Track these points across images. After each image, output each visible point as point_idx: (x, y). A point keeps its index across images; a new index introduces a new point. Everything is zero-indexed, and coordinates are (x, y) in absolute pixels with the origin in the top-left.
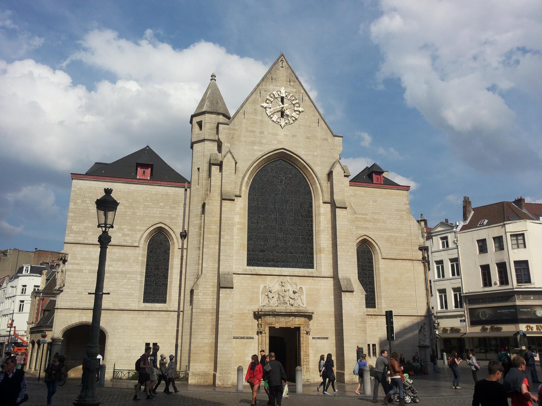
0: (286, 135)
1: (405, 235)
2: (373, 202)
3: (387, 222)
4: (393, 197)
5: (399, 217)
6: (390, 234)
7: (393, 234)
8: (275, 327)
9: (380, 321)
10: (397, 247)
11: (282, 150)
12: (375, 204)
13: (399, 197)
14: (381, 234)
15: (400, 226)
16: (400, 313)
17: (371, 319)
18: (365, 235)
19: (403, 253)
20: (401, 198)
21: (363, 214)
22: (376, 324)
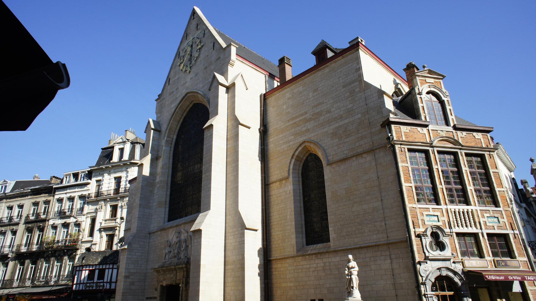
0: (191, 79)
1: (360, 116)
2: (313, 93)
3: (332, 110)
4: (338, 71)
5: (348, 94)
6: (337, 125)
7: (341, 123)
8: (163, 285)
9: (329, 262)
10: (347, 140)
11: (188, 95)
12: (315, 94)
13: (347, 66)
14: (325, 130)
15: (351, 106)
16: (358, 243)
17: (316, 260)
18: (304, 142)
19: (357, 144)
20: (351, 64)
21: (302, 115)
22: (323, 266)
